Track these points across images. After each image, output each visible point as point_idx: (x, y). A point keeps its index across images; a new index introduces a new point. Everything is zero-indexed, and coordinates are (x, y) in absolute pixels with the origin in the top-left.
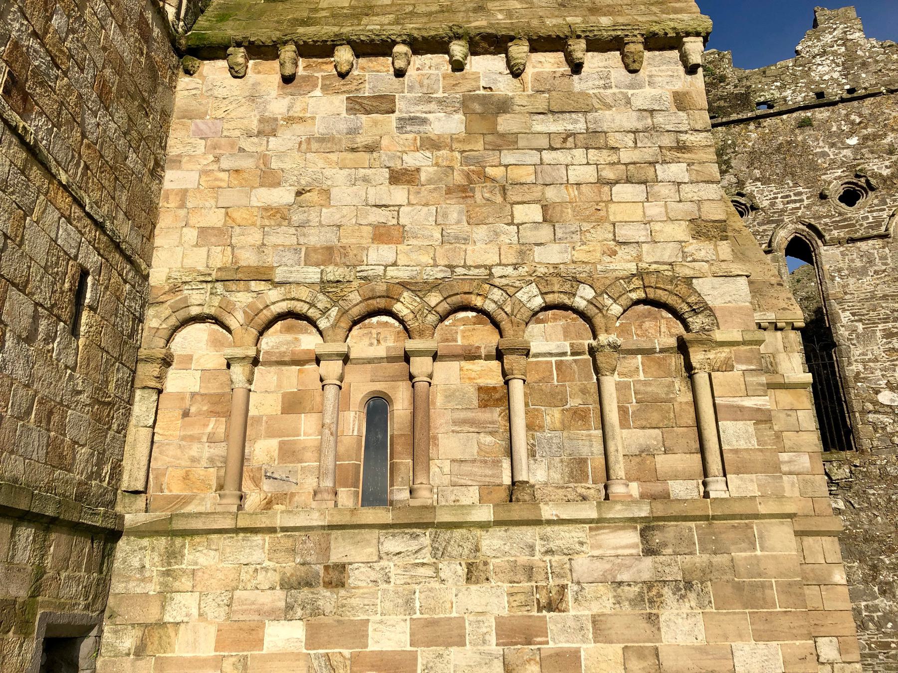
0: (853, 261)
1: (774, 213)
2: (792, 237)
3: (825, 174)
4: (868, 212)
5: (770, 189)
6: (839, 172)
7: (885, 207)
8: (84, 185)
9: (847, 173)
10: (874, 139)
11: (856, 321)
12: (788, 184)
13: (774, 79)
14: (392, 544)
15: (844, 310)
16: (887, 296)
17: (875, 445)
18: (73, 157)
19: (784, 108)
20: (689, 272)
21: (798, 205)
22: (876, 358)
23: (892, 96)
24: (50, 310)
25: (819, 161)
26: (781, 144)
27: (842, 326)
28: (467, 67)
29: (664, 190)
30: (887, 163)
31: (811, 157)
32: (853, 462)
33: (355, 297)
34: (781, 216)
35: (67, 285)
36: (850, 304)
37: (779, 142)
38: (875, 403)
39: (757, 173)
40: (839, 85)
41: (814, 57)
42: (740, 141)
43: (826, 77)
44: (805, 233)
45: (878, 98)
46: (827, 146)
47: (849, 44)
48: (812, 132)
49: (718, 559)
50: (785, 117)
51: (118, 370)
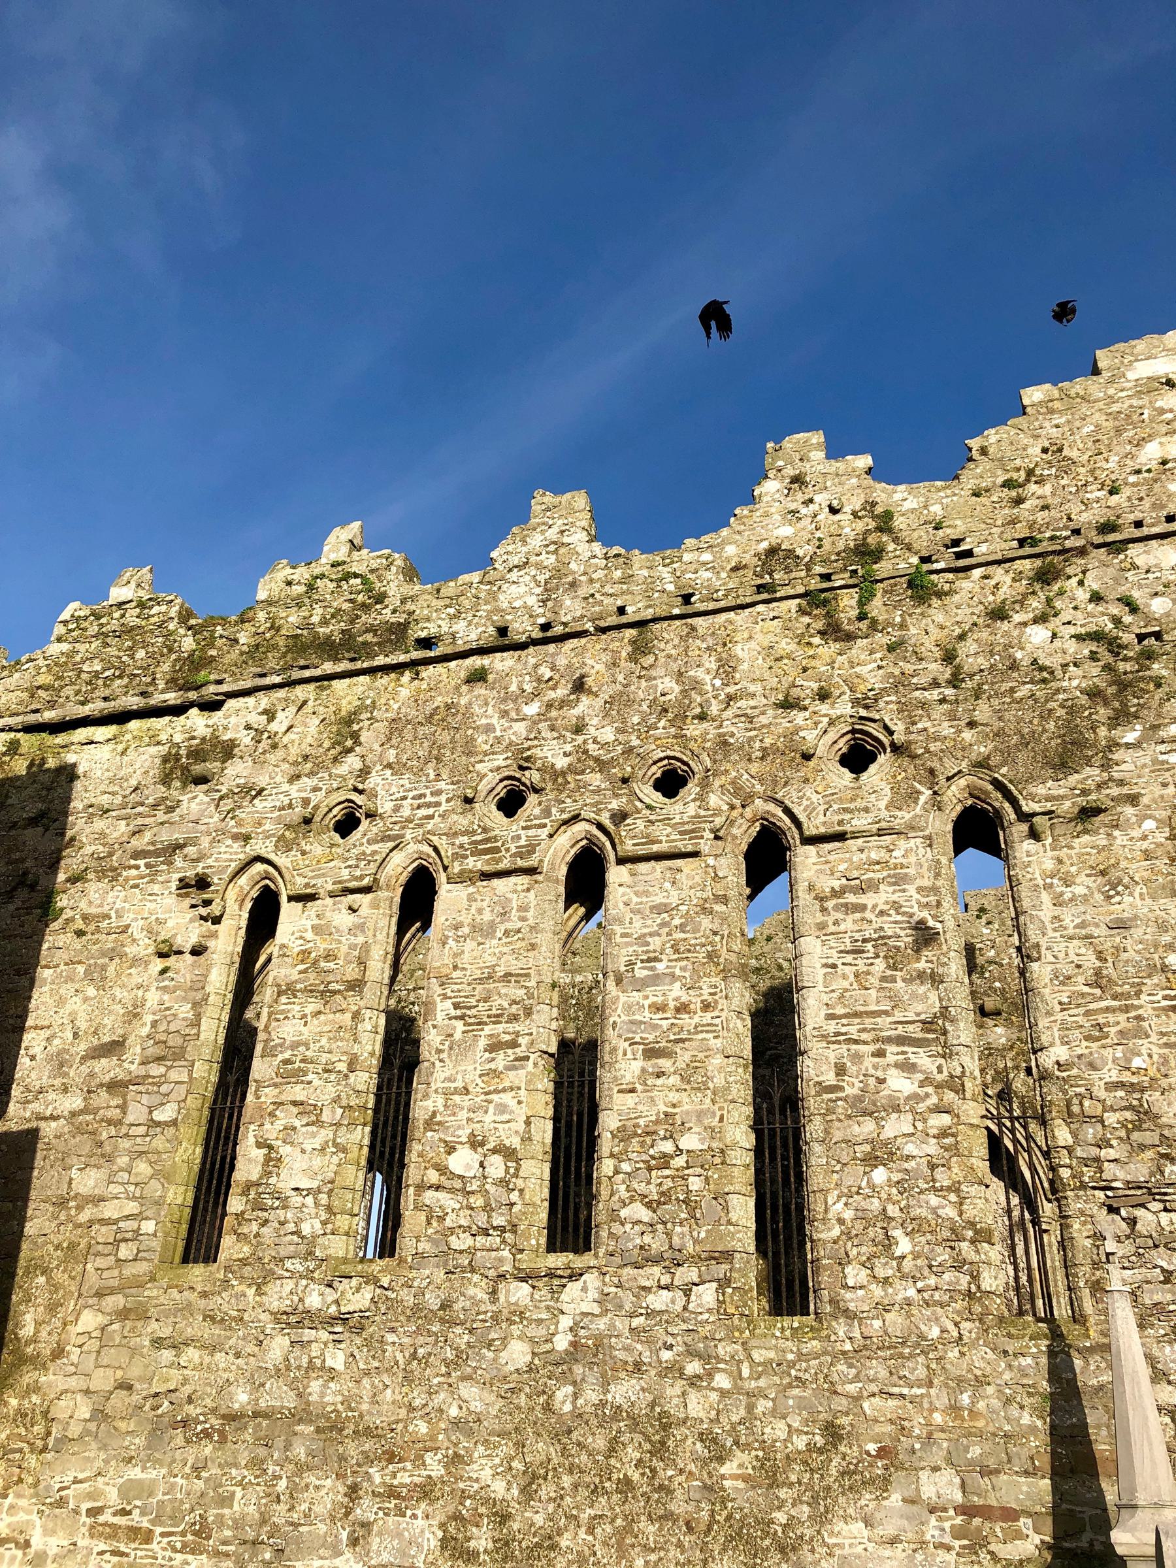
0: (480, 911)
1: (395, 823)
2: (415, 864)
3: (481, 761)
4: (524, 828)
5: (401, 782)
6: (500, 760)
7: (547, 821)
9: (509, 762)
10: (561, 708)
11: (456, 1018)
12: (428, 775)
13: (447, 602)
15: (445, 997)
16: (511, 975)
17: (420, 1250)
19: (449, 650)
21: (431, 811)
22: (465, 1088)
23: (604, 637)
25: (479, 740)
26: (438, 707)
27: (434, 1027)
30: (568, 748)
31: (470, 732)
32: (379, 1280)
34: (403, 828)
36: (455, 987)
37: (436, 704)
38: (442, 1170)
39: (391, 755)
40: (531, 616)
41: (510, 570)
42: (383, 701)
43: (517, 604)
44: (431, 860)
45: (583, 641)
46: (496, 715)
47: (562, 551)
48: (483, 691)
50: (453, 664)
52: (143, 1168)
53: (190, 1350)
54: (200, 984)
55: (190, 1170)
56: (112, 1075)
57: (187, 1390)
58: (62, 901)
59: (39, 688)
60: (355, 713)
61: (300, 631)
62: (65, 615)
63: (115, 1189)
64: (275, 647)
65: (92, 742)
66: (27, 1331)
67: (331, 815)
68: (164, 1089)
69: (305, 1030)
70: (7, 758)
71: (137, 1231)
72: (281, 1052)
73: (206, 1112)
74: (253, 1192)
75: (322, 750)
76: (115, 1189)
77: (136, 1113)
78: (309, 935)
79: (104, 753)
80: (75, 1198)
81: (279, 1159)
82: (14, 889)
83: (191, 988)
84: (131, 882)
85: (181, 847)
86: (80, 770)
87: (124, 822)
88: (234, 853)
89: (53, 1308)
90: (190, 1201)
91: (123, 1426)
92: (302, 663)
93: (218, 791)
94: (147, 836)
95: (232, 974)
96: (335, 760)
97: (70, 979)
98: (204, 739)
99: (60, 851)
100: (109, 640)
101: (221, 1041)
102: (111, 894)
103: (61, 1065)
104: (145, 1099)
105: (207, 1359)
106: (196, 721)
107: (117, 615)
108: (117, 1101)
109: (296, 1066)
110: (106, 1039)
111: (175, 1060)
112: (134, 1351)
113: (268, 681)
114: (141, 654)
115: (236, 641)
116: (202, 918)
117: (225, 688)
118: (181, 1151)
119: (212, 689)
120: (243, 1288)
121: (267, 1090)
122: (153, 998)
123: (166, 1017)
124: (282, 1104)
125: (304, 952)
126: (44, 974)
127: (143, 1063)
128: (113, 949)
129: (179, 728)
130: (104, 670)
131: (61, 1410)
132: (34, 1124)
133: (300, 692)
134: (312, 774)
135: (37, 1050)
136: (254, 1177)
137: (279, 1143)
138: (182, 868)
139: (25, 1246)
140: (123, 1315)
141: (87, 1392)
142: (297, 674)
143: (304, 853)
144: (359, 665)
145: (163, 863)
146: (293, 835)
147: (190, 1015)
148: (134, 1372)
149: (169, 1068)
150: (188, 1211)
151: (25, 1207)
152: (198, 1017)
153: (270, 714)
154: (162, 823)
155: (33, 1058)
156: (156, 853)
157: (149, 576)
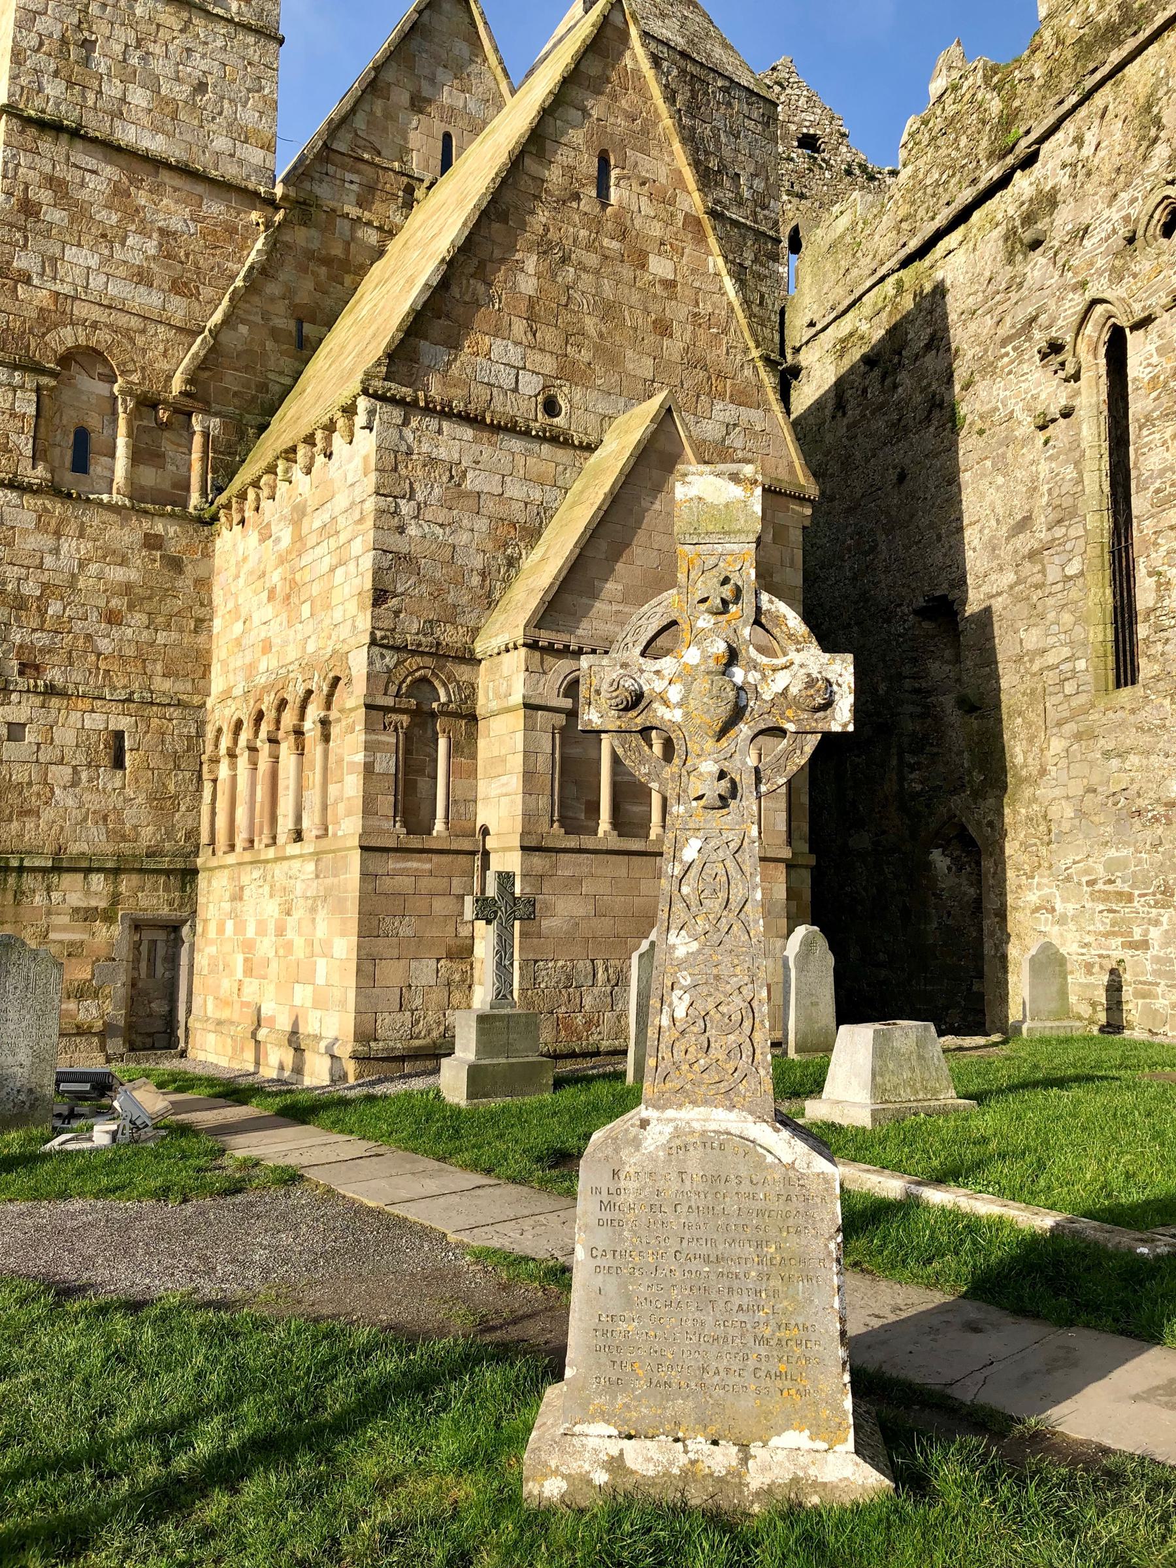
8: (107, 682)
14: (256, 874)
18: (91, 673)
20: (346, 648)
24: (89, 765)
28: (293, 479)
29: (352, 566)
33: (252, 702)
35: (102, 746)
49: (336, 880)
51: (176, 775)
52: (1067, 618)
53: (1131, 757)
54: (1075, 444)
55: (1104, 611)
56: (1029, 546)
57: (1135, 787)
58: (963, 410)
59: (901, 222)
60: (1152, 94)
61: (1082, 31)
62: (905, 138)
63: (1051, 640)
64: (1065, 64)
65: (950, 252)
66: (1019, 760)
67: (1154, 221)
68: (1069, 546)
69: (1167, 455)
70: (898, 299)
71: (1073, 670)
72: (1152, 483)
73: (1107, 556)
74: (1152, 617)
75: (1130, 154)
76: (1051, 640)
77: (1053, 574)
78: (1155, 360)
79: (959, 258)
80: (1027, 654)
81: (1168, 583)
82: (930, 412)
83: (1070, 450)
84: (1006, 370)
85: (1034, 319)
86: (948, 284)
87: (989, 316)
88: (1075, 303)
89: (1031, 740)
90: (1110, 636)
91: (1096, 819)
92: (1091, 66)
93: (1052, 248)
94: (1008, 321)
95: (1103, 423)
96: (1145, 158)
97: (983, 475)
98: (1031, 200)
99: (951, 365)
100: (938, 143)
101: (1107, 489)
102: (995, 387)
103: (993, 550)
104: (1056, 559)
105: (1145, 762)
106: (1023, 183)
107: (938, 112)
108: (1038, 567)
109: (1166, 492)
110: (1019, 517)
111: (1071, 519)
112: (1092, 764)
113: (1067, 106)
114: (963, 141)
115: (1032, 78)
116: (1066, 380)
117: (1033, 136)
118: (1091, 596)
119: (1023, 143)
120: (1160, 700)
121: (1147, 522)
122: (1044, 468)
123: (1056, 483)
124: (1161, 531)
125: (1153, 378)
126: (965, 477)
127: (1049, 529)
128: (1006, 437)
129: (1010, 200)
130: (941, 175)
131: (1054, 812)
132: (987, 604)
133: (1099, 99)
134: (1127, 185)
135: (976, 543)
136: (1151, 604)
137: (1166, 567)
138: (1040, 338)
139: (1003, 697)
140: (1078, 737)
141: (1068, 798)
142: (1089, 82)
143: (1135, 276)
144: (1142, 36)
145: (1025, 341)
146: (1122, 261)
147: (1075, 475)
148: (1095, 779)
149: (1068, 527)
150: (1110, 645)
151: (997, 668)
152: (1080, 474)
153: (1079, 141)
154: (1016, 303)
155: (974, 550)
156: (1017, 335)
157: (959, 50)
